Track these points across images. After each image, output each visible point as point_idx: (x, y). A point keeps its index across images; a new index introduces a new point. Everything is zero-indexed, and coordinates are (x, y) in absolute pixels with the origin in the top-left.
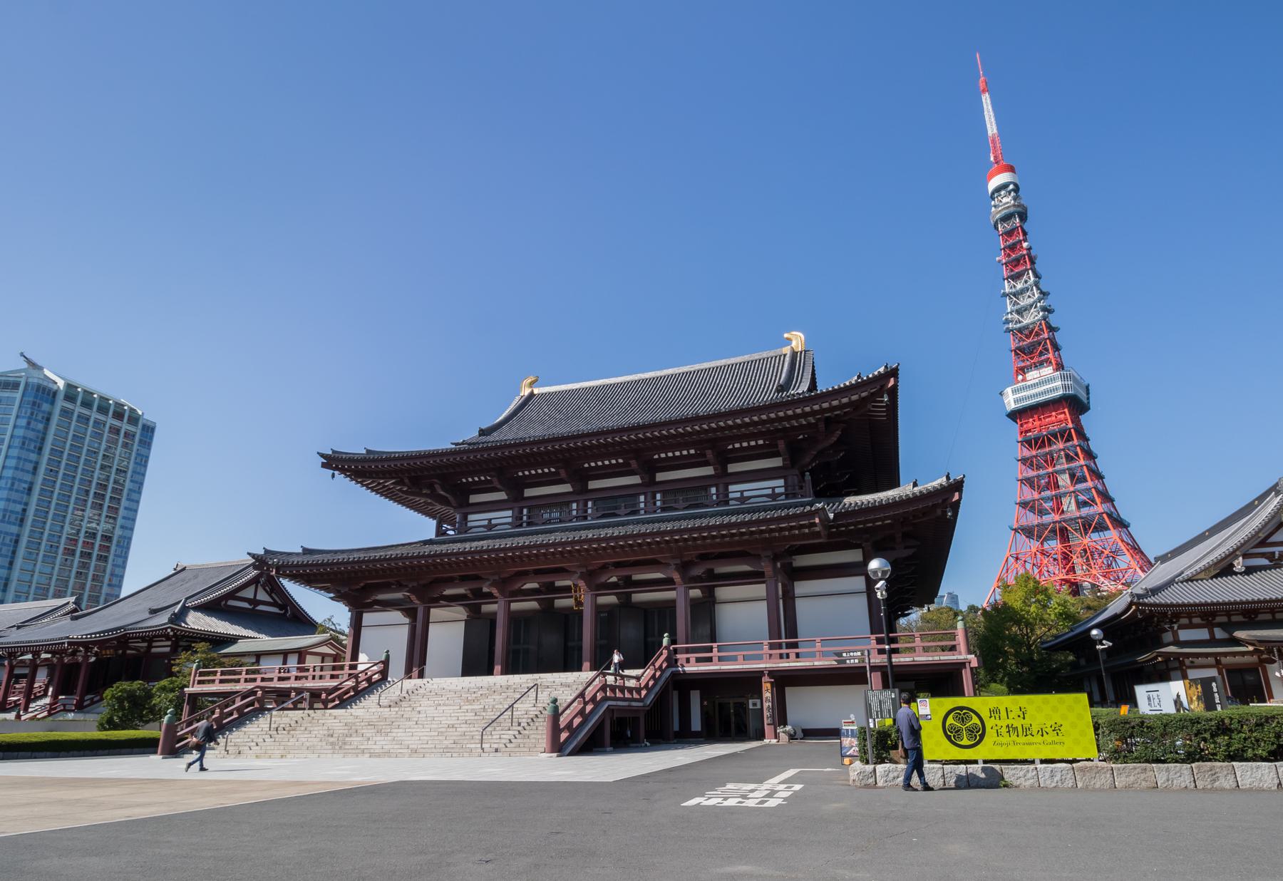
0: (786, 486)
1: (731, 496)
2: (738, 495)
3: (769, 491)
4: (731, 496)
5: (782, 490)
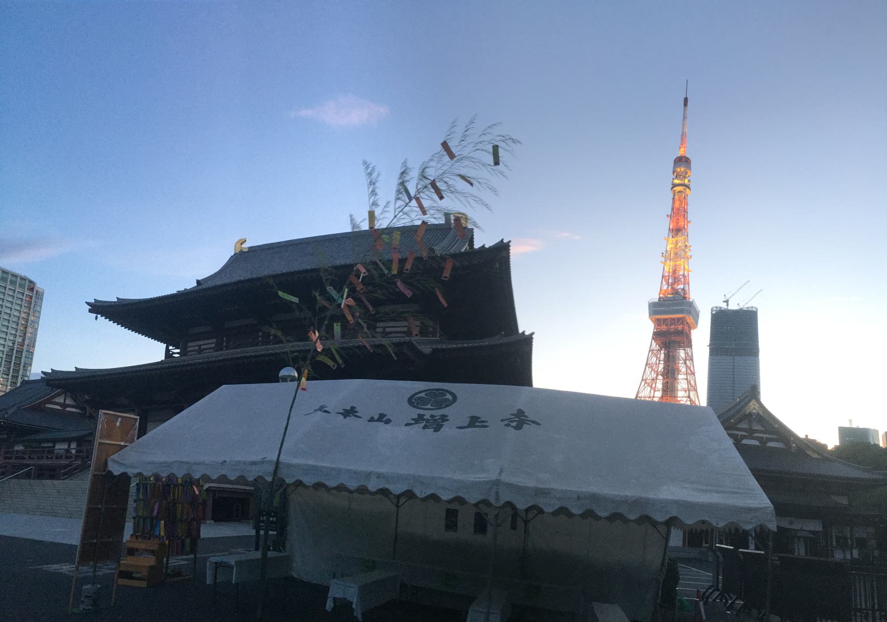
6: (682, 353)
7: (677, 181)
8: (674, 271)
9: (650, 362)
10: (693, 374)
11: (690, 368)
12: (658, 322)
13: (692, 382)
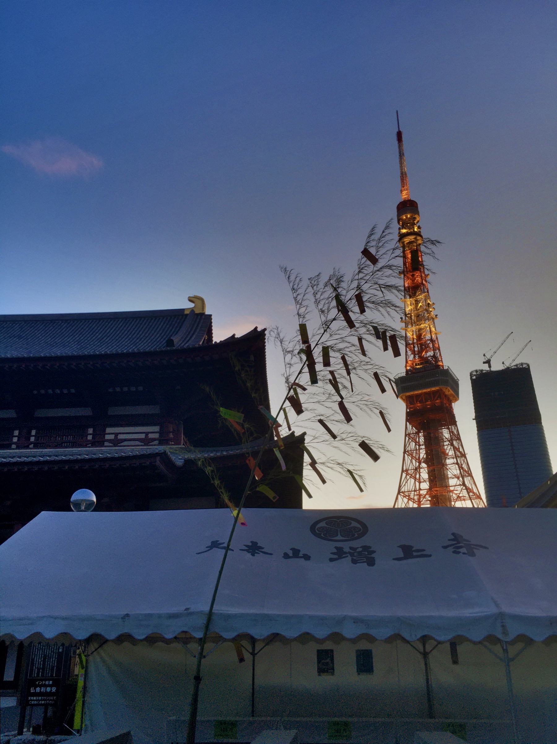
0: (161, 433)
1: (107, 437)
2: (112, 437)
3: (143, 436)
4: (107, 437)
5: (157, 436)
6: (446, 434)
7: (404, 231)
8: (419, 337)
9: (408, 449)
10: (464, 455)
11: (458, 450)
12: (409, 401)
13: (464, 466)
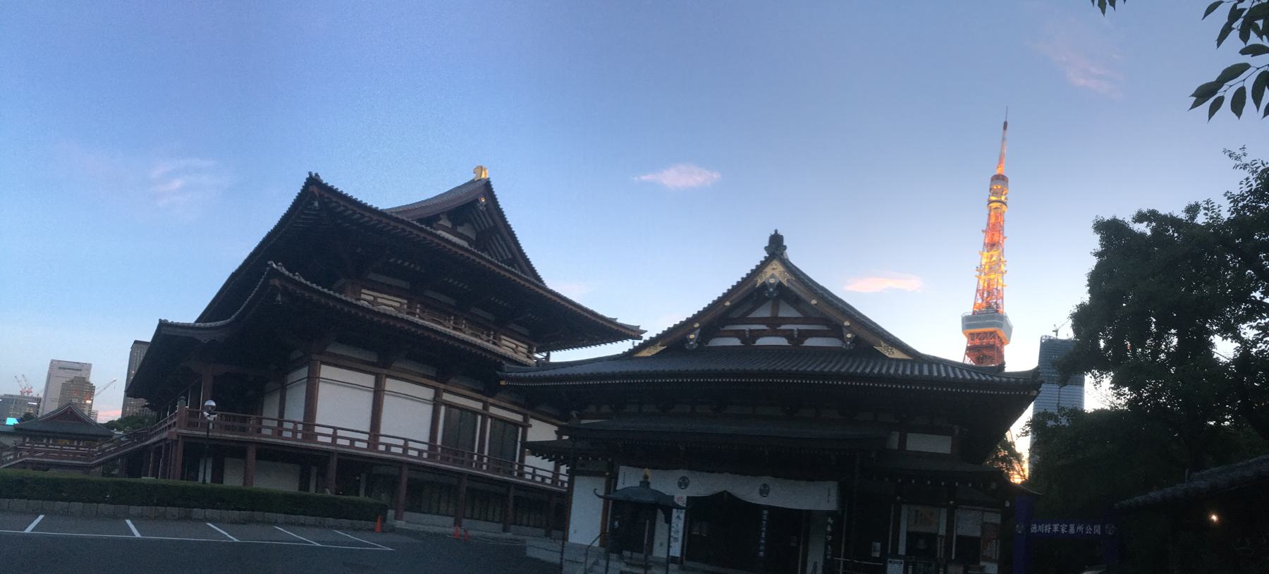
7: (993, 198)
12: (971, 336)
